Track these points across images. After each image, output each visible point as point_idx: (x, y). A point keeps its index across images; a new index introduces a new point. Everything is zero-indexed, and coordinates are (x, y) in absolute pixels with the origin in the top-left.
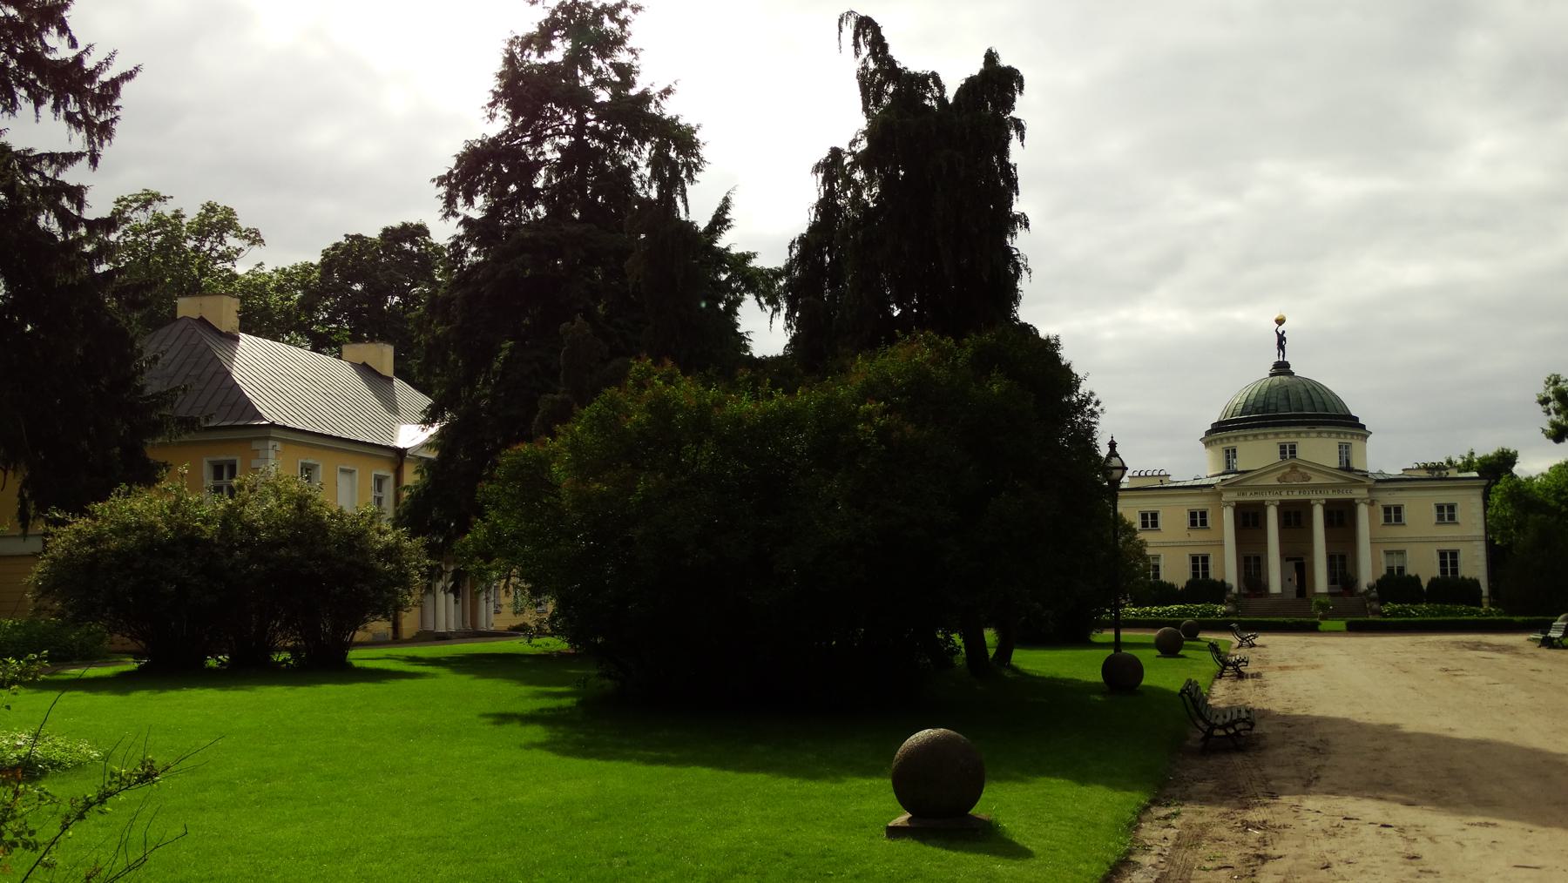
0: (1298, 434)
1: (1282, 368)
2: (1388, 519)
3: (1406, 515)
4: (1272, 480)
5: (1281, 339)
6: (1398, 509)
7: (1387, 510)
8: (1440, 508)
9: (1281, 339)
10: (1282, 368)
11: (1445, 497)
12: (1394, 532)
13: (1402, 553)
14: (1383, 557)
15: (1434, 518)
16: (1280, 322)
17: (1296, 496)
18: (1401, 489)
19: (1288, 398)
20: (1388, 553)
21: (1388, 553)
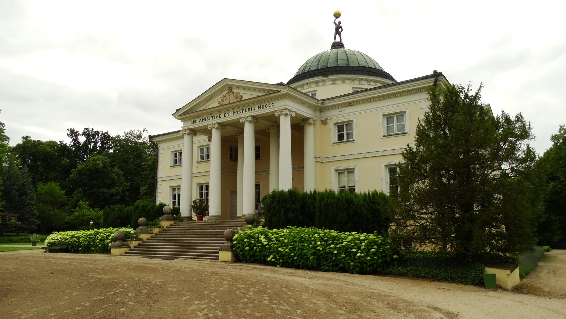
0: (317, 83)
1: (338, 45)
2: (341, 137)
3: (356, 132)
4: (214, 104)
5: (338, 29)
6: (349, 124)
7: (340, 128)
8: (388, 118)
9: (338, 29)
10: (338, 45)
11: (392, 106)
12: (345, 149)
13: (351, 171)
14: (334, 177)
15: (383, 130)
16: (337, 15)
17: (231, 117)
18: (350, 104)
19: (319, 61)
20: (340, 172)
21: (340, 172)
